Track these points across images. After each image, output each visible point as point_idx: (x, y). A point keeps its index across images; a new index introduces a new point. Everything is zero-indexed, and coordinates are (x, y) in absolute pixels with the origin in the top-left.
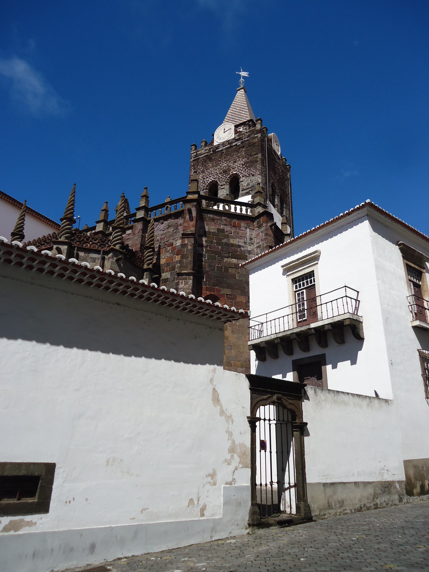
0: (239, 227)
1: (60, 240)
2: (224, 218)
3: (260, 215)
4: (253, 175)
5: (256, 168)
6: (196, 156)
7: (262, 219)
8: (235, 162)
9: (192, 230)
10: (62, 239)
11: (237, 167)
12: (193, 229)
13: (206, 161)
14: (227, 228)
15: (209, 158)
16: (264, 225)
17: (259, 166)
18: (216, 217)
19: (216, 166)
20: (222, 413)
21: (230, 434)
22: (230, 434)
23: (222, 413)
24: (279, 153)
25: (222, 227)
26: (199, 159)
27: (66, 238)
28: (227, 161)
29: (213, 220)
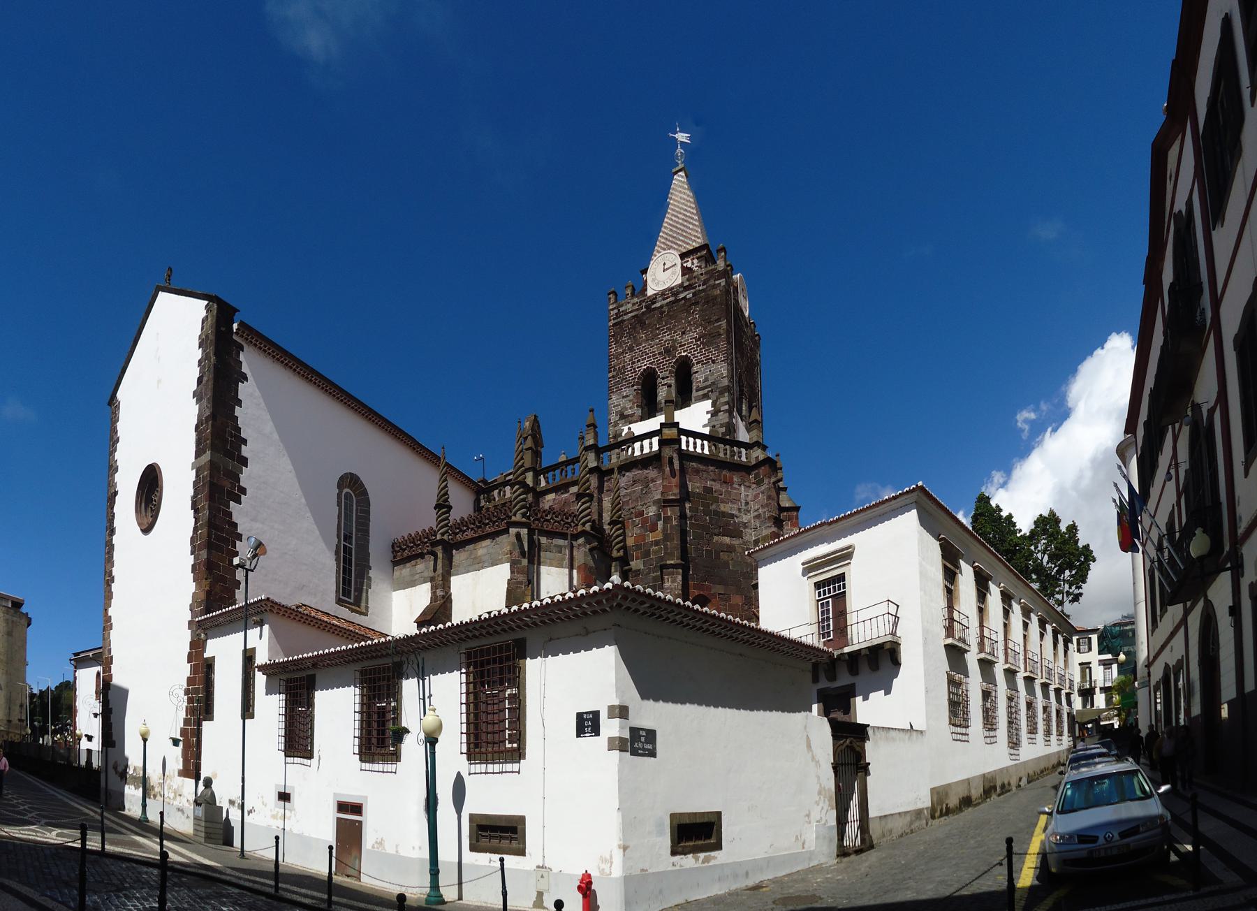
0: (731, 483)
1: (514, 518)
2: (711, 468)
3: (759, 464)
4: (714, 362)
5: (718, 348)
6: (618, 315)
7: (762, 470)
8: (683, 333)
9: (674, 494)
10: (518, 518)
11: (687, 343)
12: (676, 491)
13: (634, 328)
14: (716, 486)
15: (639, 321)
16: (766, 481)
17: (723, 345)
18: (701, 467)
19: (652, 339)
20: (813, 758)
21: (818, 777)
22: (818, 777)
23: (813, 758)
24: (747, 314)
25: (709, 484)
26: (622, 321)
27: (524, 515)
28: (670, 329)
29: (697, 471)
